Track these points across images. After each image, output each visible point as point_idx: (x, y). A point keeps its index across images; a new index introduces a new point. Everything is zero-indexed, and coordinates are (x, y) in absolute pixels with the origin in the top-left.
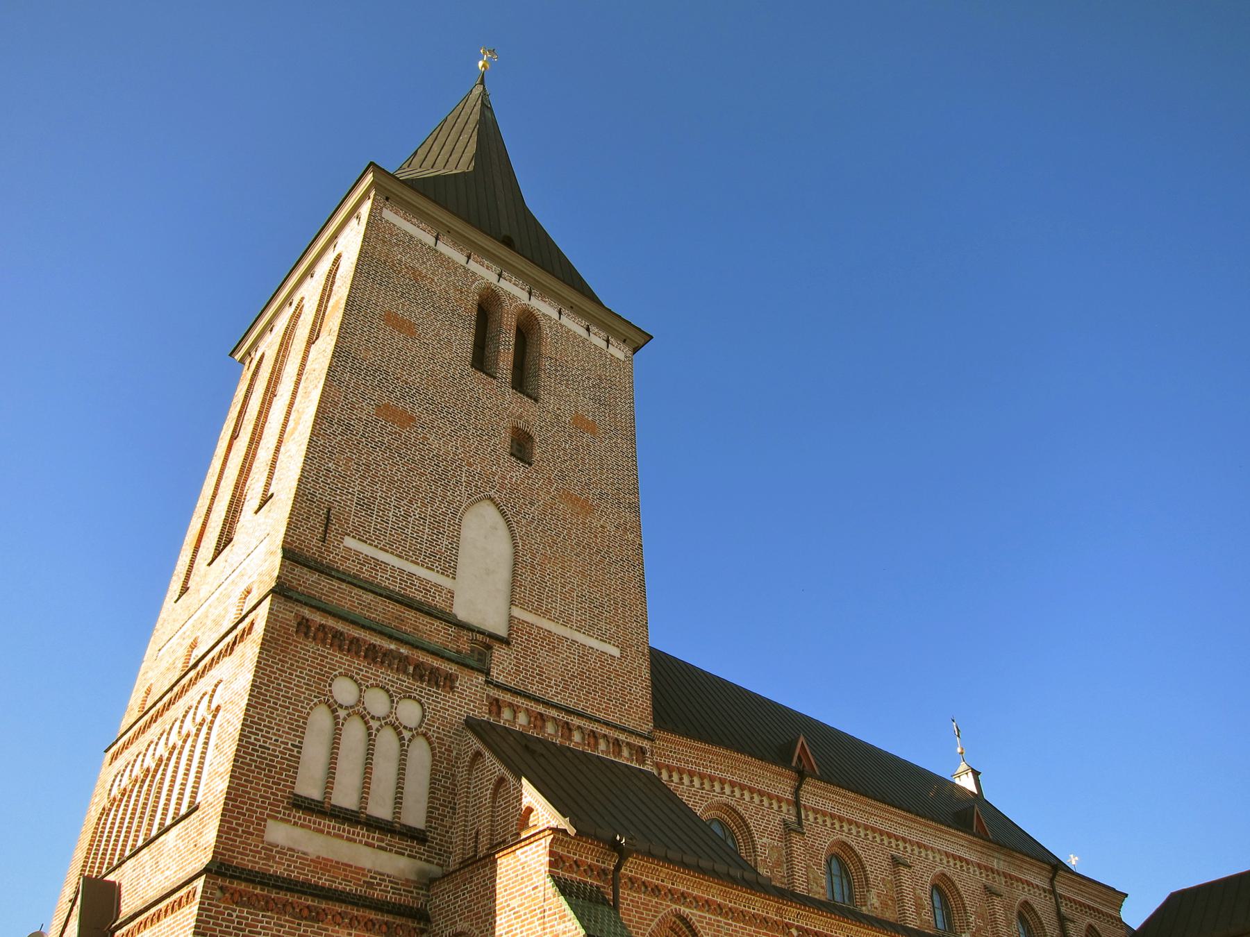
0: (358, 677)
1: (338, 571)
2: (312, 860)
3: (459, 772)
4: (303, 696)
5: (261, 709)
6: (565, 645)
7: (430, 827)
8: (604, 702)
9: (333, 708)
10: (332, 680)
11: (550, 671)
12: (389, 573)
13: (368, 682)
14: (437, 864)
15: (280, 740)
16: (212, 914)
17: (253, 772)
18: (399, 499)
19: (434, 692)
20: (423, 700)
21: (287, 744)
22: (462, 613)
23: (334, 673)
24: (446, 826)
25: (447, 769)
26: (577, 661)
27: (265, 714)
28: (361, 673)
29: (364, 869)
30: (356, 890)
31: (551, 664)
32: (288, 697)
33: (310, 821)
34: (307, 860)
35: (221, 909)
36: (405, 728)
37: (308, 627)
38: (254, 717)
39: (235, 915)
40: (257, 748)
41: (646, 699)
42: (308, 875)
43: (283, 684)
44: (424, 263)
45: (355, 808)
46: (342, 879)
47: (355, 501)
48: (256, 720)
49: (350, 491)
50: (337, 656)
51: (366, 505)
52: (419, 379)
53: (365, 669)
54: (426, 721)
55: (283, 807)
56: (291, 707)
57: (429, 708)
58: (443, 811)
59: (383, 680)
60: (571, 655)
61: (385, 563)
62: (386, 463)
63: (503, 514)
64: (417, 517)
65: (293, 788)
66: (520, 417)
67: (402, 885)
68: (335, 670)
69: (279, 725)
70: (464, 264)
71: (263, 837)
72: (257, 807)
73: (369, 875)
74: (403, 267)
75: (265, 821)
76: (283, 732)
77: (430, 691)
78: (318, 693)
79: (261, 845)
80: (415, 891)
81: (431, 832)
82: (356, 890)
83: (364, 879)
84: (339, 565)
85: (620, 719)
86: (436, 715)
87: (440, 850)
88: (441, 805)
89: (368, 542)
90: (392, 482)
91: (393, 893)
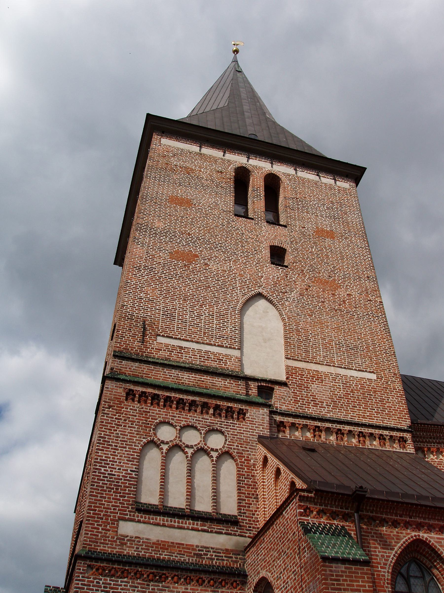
0: (173, 421)
2: (154, 543)
3: (257, 473)
4: (135, 438)
5: (106, 451)
6: (331, 378)
8: (368, 411)
11: (321, 397)
12: (191, 354)
13: (180, 423)
15: (122, 468)
16: (86, 583)
17: (105, 491)
18: (192, 307)
19: (231, 423)
20: (223, 430)
21: (127, 470)
22: (248, 372)
24: (252, 511)
25: (248, 472)
26: (341, 387)
27: (110, 453)
28: (175, 418)
29: (193, 545)
30: (189, 559)
31: (321, 392)
32: (124, 441)
33: (149, 518)
34: (150, 543)
35: (91, 579)
38: (102, 456)
39: (101, 582)
40: (107, 475)
41: (402, 404)
42: (152, 553)
43: (120, 433)
44: (192, 162)
45: (183, 507)
46: (177, 554)
48: (104, 458)
50: (156, 410)
52: (197, 231)
53: (177, 415)
56: (127, 446)
57: (228, 434)
59: (192, 421)
60: (336, 384)
61: (187, 348)
62: (180, 286)
63: (270, 302)
64: (207, 315)
68: (157, 419)
69: (120, 459)
71: (117, 532)
72: (111, 512)
73: (197, 549)
74: (179, 168)
76: (124, 463)
77: (227, 422)
78: (145, 435)
80: (234, 556)
81: (241, 516)
82: (189, 559)
84: (154, 355)
85: (383, 421)
86: (234, 438)
87: (250, 527)
88: (246, 497)
91: (217, 559)
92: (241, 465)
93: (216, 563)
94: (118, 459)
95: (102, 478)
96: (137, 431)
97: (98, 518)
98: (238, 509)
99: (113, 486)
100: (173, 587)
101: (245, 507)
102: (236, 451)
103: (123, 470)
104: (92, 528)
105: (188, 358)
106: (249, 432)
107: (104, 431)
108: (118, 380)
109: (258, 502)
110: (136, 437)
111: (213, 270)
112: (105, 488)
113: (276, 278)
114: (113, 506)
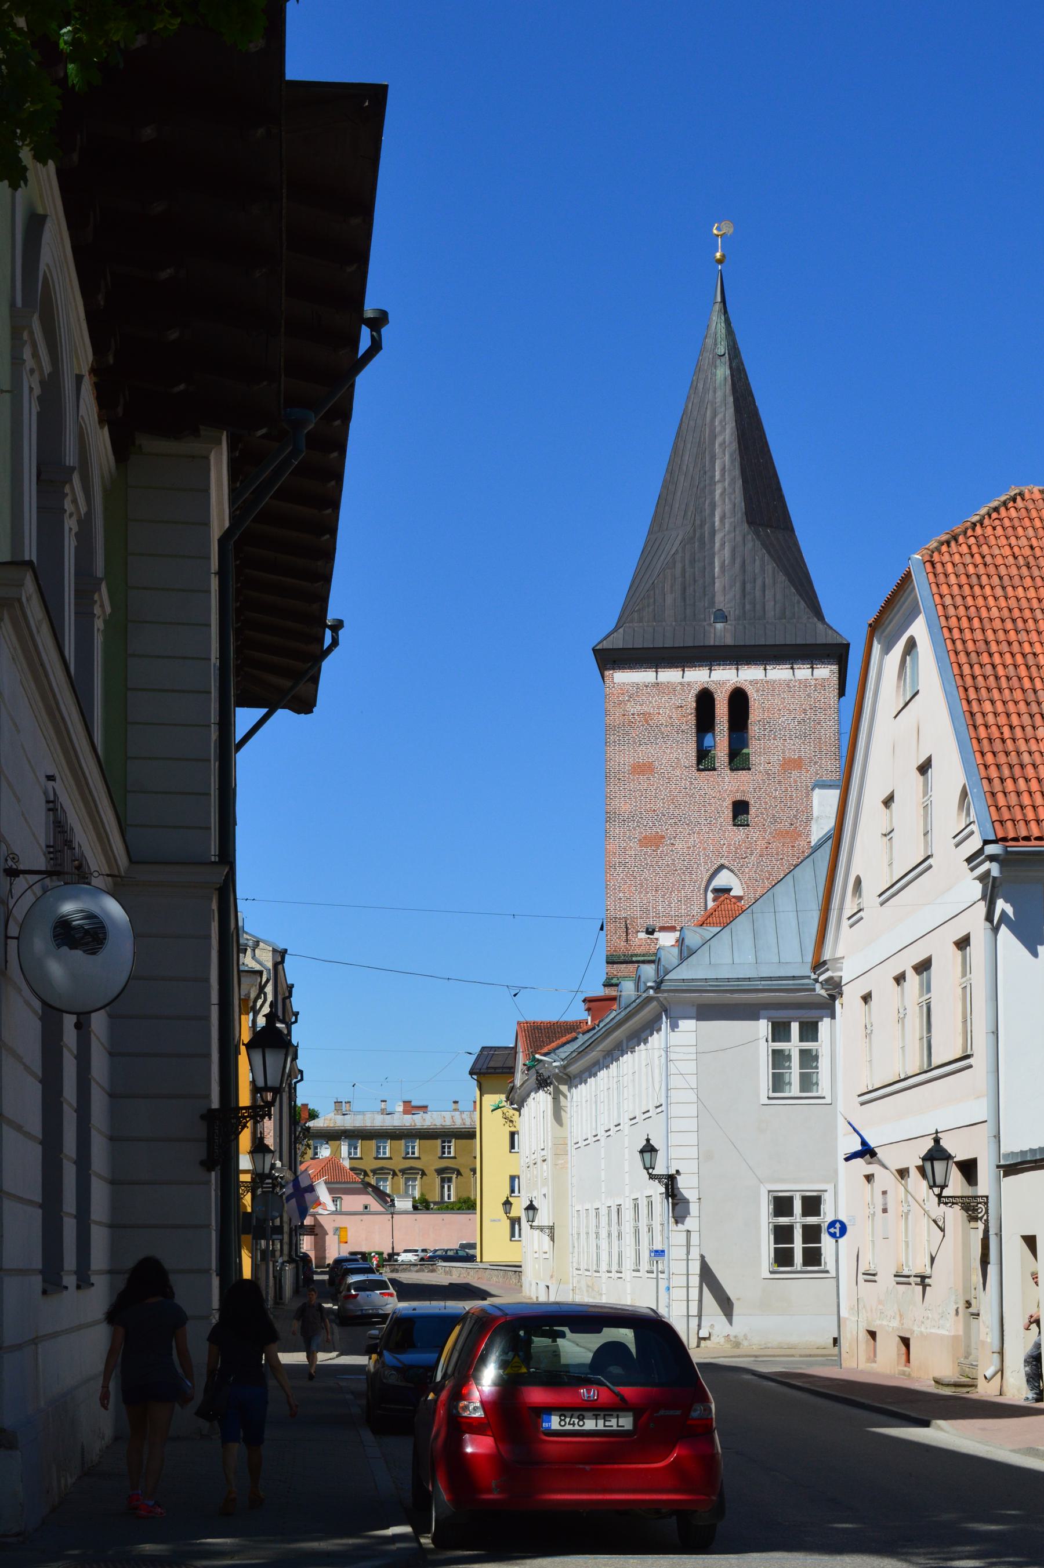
63: (732, 871)
66: (737, 791)
113: (737, 843)
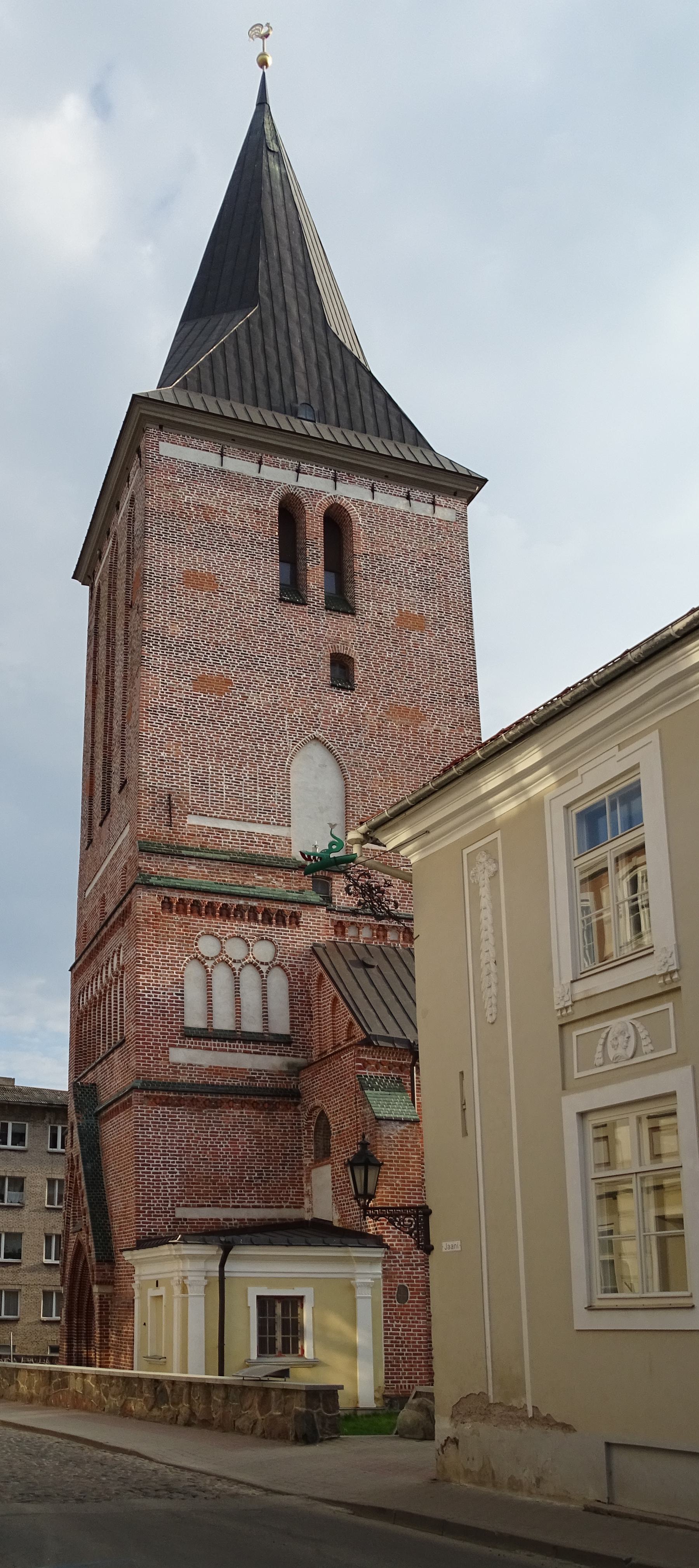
0: (217, 933)
1: (187, 849)
2: (206, 1069)
3: (311, 988)
7: (293, 1032)
9: (201, 960)
10: (197, 940)
12: (231, 837)
13: (225, 935)
14: (302, 1057)
15: (166, 992)
17: (152, 1018)
19: (282, 930)
23: (198, 934)
24: (306, 1030)
27: (152, 976)
29: (246, 1069)
30: (242, 1083)
33: (200, 1044)
34: (203, 1069)
36: (262, 963)
37: (170, 903)
38: (144, 980)
39: (159, 1111)
43: (159, 951)
45: (233, 1029)
47: (190, 781)
48: (146, 982)
49: (184, 773)
50: (197, 921)
51: (201, 782)
52: (228, 636)
54: (279, 954)
55: (179, 1038)
58: (303, 1019)
64: (248, 779)
65: (183, 1024)
67: (277, 1075)
68: (198, 932)
69: (164, 982)
70: (256, 475)
71: (168, 1060)
72: (160, 1041)
75: (168, 1049)
76: (168, 986)
78: (188, 952)
79: (168, 1066)
81: (294, 1036)
82: (242, 1083)
83: (246, 1075)
88: (299, 1015)
89: (208, 814)
90: (219, 752)
91: (271, 1082)
92: (294, 980)
93: (269, 1085)
94: (161, 982)
95: (146, 1004)
96: (178, 948)
97: (148, 1047)
98: (291, 1028)
99: (159, 1013)
100: (229, 1112)
101: (298, 1025)
102: (288, 964)
103: (168, 994)
104: (143, 1058)
105: (227, 844)
106: (303, 940)
107: (143, 951)
108: (150, 886)
109: (312, 1019)
110: (177, 955)
111: (253, 705)
112: (151, 1015)
114: (161, 1033)
